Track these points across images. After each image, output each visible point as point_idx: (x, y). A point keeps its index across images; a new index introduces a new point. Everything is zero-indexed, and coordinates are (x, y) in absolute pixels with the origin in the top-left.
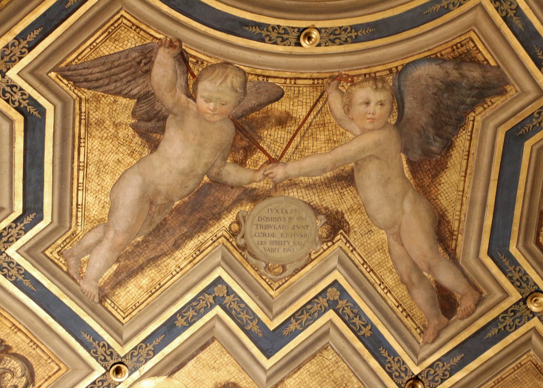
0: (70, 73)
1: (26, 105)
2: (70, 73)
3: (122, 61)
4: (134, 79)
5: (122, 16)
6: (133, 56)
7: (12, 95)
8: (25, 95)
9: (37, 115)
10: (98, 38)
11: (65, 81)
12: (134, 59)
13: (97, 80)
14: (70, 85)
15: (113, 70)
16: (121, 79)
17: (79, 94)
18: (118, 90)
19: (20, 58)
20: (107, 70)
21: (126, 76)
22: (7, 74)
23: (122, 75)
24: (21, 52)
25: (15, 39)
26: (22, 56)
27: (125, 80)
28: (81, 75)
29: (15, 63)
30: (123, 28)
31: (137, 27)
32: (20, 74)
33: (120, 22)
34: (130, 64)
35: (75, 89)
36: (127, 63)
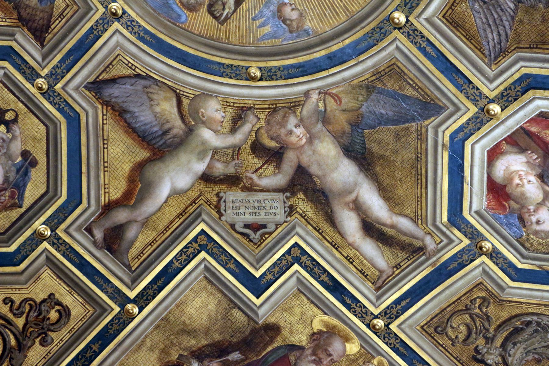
0: (493, 55)
1: (520, 87)
2: (493, 55)
3: (482, 16)
4: (500, 6)
5: (443, 17)
6: (478, 7)
7: (511, 96)
8: (510, 87)
9: (530, 80)
10: (462, 34)
11: (499, 59)
12: (481, 7)
13: (499, 35)
14: (504, 55)
15: (491, 23)
16: (499, 16)
17: (512, 48)
18: (510, 19)
19: (478, 89)
20: (490, 28)
21: (497, 13)
22: (491, 98)
23: (496, 16)
24: (472, 89)
25: (461, 92)
26: (476, 87)
27: (501, 13)
28: (494, 47)
29: (482, 93)
30: (454, 16)
31: (453, 5)
32: (491, 90)
33: (448, 18)
34: (485, 10)
35: (507, 51)
36: (484, 12)
